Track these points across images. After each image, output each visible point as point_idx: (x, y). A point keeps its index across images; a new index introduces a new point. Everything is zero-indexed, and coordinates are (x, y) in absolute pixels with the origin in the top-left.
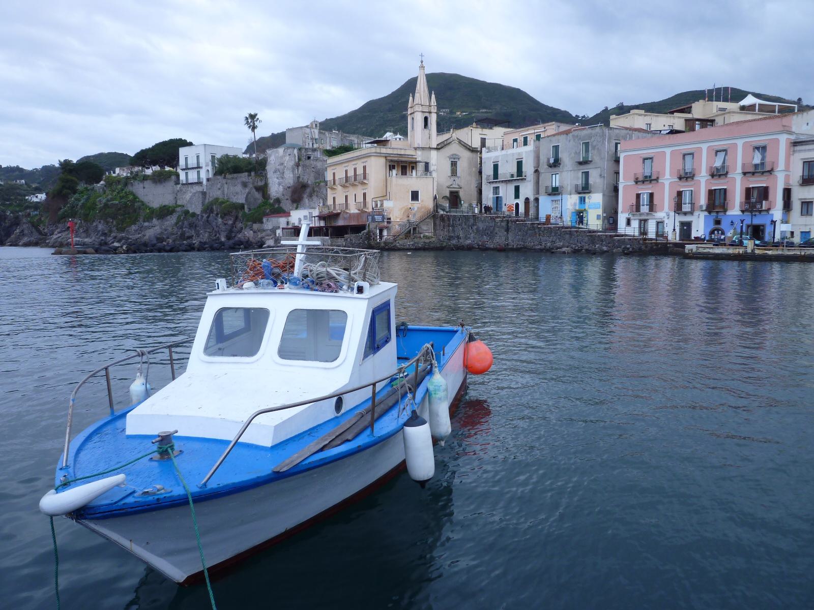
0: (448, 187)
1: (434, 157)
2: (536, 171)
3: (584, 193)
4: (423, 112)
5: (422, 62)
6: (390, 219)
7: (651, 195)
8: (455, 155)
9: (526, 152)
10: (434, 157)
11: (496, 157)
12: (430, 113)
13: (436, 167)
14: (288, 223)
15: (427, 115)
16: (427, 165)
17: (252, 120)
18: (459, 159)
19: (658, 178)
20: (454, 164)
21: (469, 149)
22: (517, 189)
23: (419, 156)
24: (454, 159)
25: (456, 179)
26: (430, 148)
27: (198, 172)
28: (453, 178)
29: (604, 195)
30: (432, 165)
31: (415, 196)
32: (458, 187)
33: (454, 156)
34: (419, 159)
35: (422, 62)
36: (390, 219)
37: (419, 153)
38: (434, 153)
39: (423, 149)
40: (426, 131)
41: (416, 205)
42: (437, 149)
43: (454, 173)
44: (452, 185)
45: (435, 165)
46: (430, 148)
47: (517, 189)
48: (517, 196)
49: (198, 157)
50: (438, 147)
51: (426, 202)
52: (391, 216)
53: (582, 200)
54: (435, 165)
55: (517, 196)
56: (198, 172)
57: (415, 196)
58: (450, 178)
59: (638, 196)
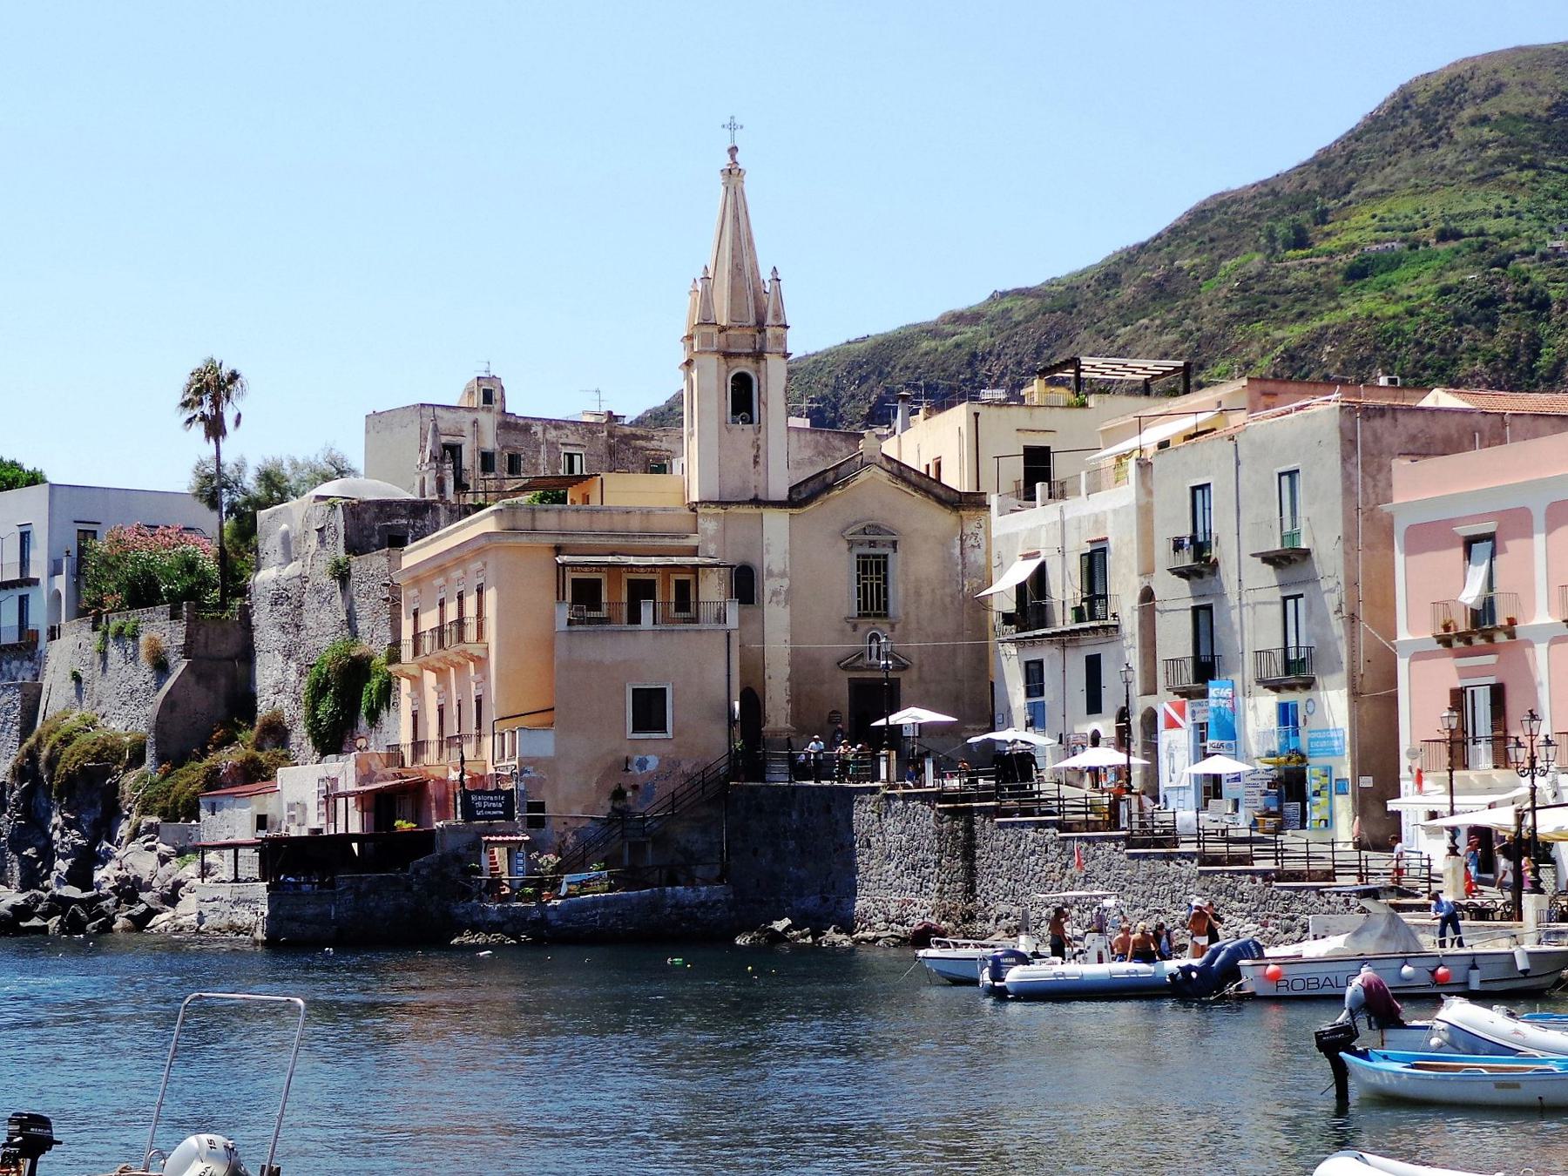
2: (1147, 595)
3: (1292, 688)
5: (733, 150)
6: (540, 807)
7: (1498, 694)
9: (1115, 512)
11: (1033, 532)
14: (262, 822)
15: (745, 366)
16: (744, 583)
17: (211, 394)
18: (894, 544)
19: (1512, 622)
22: (1093, 664)
25: (882, 626)
27: (23, 601)
28: (865, 626)
29: (1355, 695)
30: (771, 574)
31: (649, 709)
35: (733, 150)
36: (540, 807)
38: (776, 523)
40: (744, 433)
41: (652, 752)
43: (873, 595)
45: (783, 575)
46: (756, 502)
47: (1093, 664)
48: (1094, 706)
49: (25, 538)
51: (697, 737)
52: (545, 796)
53: (1286, 715)
54: (783, 575)
55: (1094, 706)
56: (23, 601)
57: (649, 709)
58: (855, 628)
59: (1458, 698)
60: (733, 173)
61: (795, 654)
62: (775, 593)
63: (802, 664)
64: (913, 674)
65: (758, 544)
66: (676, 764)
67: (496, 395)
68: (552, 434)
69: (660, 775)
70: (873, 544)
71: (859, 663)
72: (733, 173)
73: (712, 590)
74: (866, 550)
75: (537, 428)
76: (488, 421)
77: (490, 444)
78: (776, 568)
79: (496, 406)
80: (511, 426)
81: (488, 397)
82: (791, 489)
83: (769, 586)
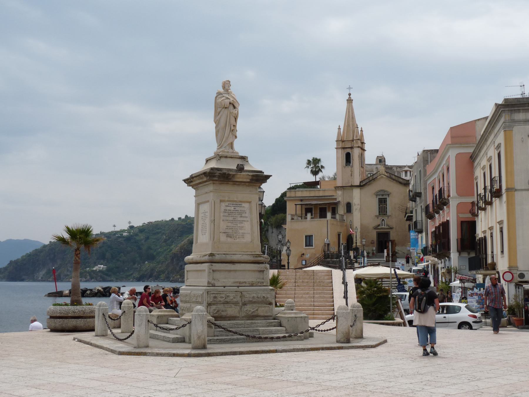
0: (376, 228)
1: (356, 197)
4: (344, 148)
5: (350, 95)
8: (382, 190)
10: (356, 197)
12: (352, 148)
16: (349, 207)
18: (388, 195)
20: (382, 202)
21: (400, 183)
23: (340, 196)
24: (383, 195)
25: (385, 218)
26: (352, 186)
30: (355, 205)
31: (309, 241)
32: (388, 227)
33: (382, 193)
34: (339, 199)
35: (350, 95)
37: (339, 193)
38: (356, 192)
39: (343, 188)
40: (348, 169)
42: (361, 186)
44: (379, 225)
50: (362, 184)
57: (309, 241)
58: (378, 218)
60: (350, 101)
61: (361, 225)
62: (356, 209)
63: (363, 228)
64: (394, 230)
66: (315, 254)
68: (399, 169)
69: (310, 258)
70: (383, 195)
71: (379, 227)
73: (341, 210)
74: (381, 197)
75: (395, 169)
78: (356, 203)
80: (389, 169)
81: (380, 161)
82: (360, 182)
83: (355, 208)
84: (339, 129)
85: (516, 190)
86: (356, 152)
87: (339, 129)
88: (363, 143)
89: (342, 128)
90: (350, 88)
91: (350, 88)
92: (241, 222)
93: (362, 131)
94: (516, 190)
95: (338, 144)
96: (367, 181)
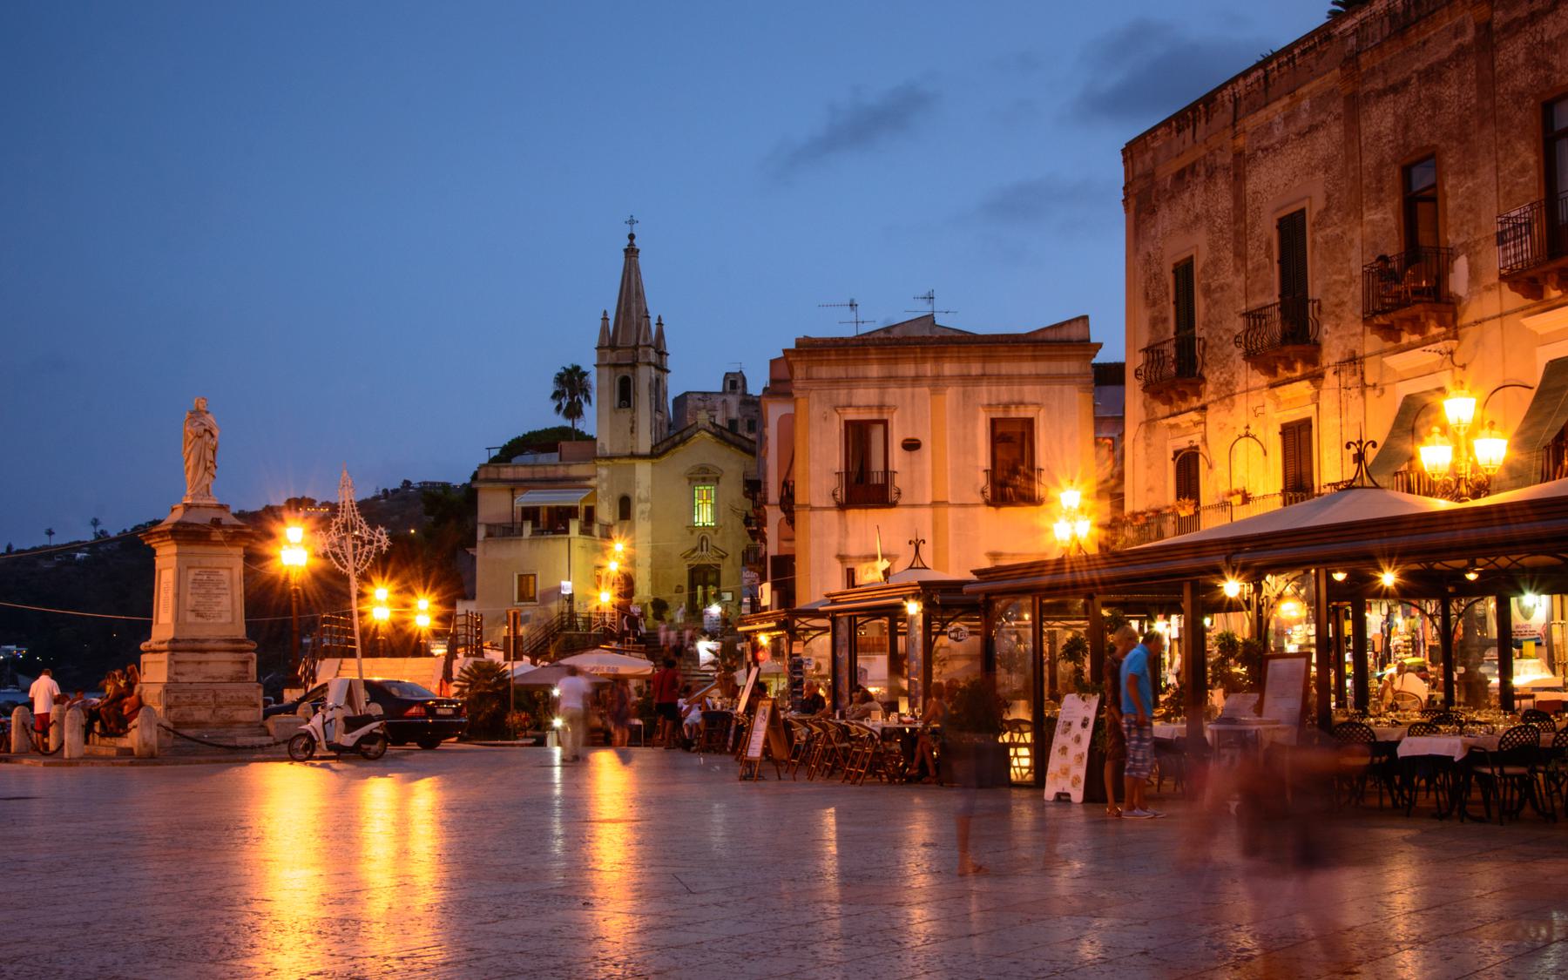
5: (632, 237)
13: (649, 505)
15: (626, 371)
35: (632, 237)
38: (643, 470)
40: (625, 415)
42: (654, 455)
45: (646, 501)
46: (633, 456)
60: (631, 252)
62: (643, 512)
65: (631, 482)
67: (740, 384)
72: (631, 252)
76: (733, 401)
77: (734, 414)
79: (739, 391)
81: (734, 385)
83: (638, 509)
84: (605, 319)
85: (813, 509)
86: (645, 375)
87: (605, 319)
88: (662, 354)
89: (612, 316)
90: (631, 222)
91: (631, 222)
92: (217, 596)
93: (660, 324)
94: (813, 509)
95: (601, 356)
96: (666, 445)
